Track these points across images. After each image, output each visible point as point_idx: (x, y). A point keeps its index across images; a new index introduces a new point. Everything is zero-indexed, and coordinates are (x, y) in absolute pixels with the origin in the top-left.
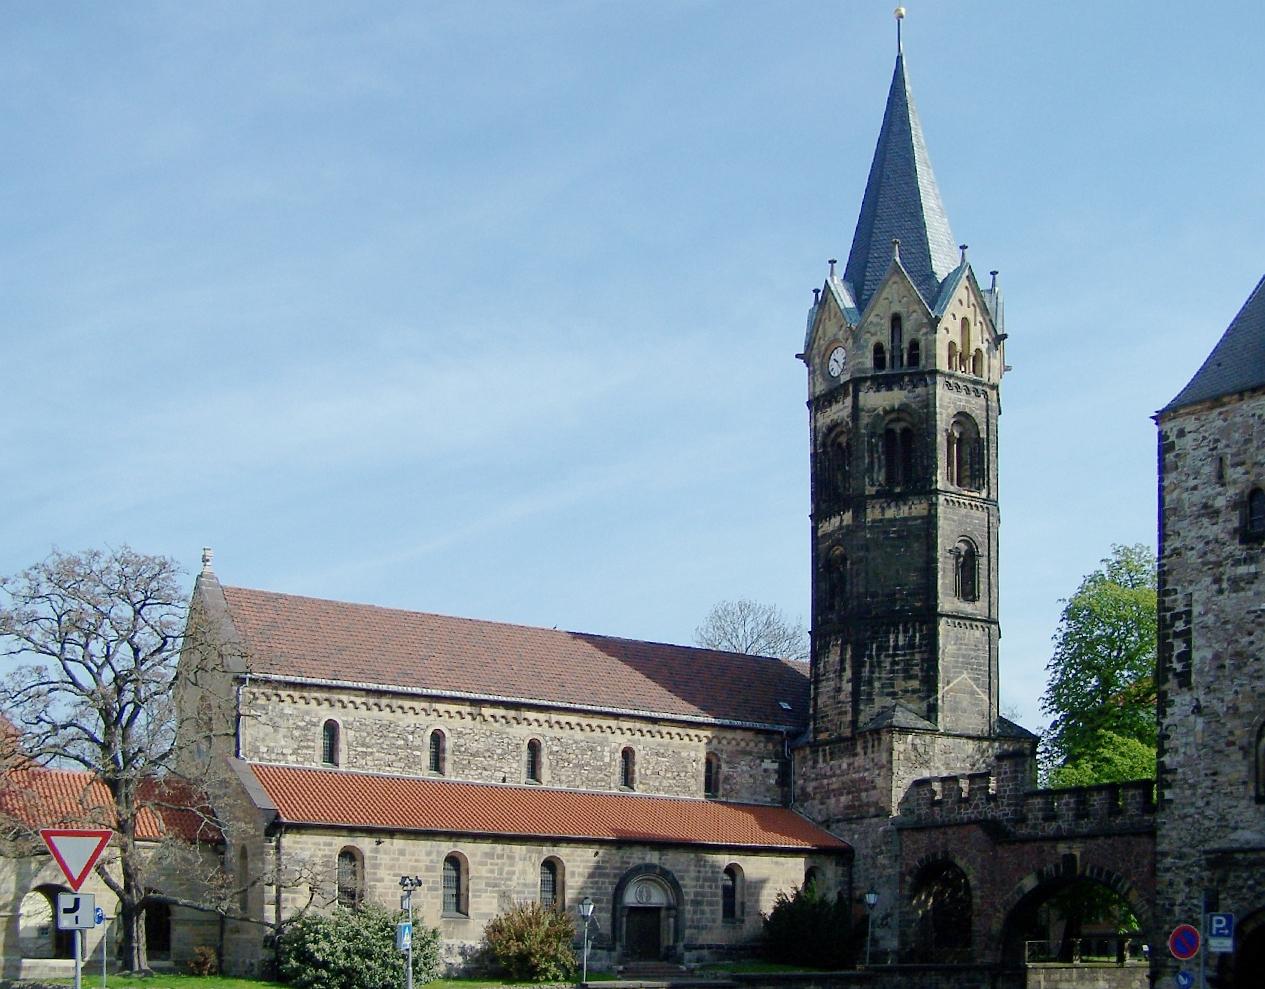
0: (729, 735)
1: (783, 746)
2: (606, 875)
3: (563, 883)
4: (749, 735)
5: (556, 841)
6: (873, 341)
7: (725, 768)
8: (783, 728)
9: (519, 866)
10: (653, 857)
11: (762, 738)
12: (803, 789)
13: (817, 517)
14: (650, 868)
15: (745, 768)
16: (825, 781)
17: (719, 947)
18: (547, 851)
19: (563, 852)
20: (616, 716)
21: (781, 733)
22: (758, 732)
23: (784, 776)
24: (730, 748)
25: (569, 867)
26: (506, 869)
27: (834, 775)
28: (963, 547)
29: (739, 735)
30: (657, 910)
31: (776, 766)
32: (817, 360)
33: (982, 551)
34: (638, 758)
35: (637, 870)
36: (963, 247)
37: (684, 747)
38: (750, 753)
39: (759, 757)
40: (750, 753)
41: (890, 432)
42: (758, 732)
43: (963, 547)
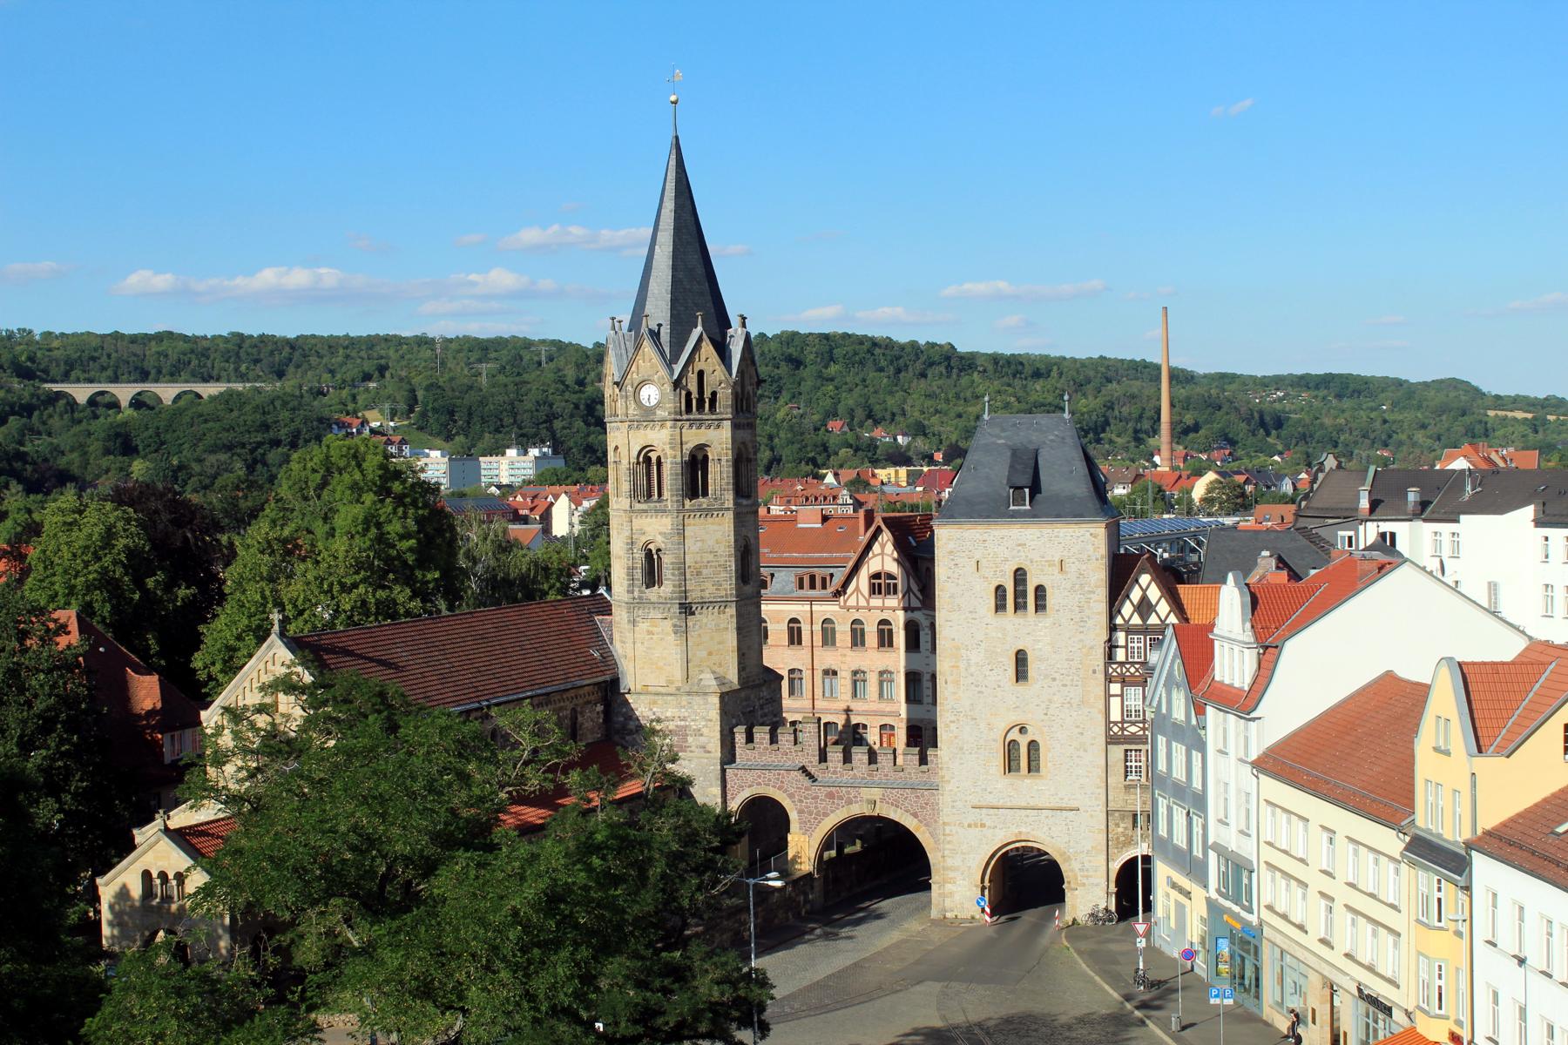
32: (629, 388)
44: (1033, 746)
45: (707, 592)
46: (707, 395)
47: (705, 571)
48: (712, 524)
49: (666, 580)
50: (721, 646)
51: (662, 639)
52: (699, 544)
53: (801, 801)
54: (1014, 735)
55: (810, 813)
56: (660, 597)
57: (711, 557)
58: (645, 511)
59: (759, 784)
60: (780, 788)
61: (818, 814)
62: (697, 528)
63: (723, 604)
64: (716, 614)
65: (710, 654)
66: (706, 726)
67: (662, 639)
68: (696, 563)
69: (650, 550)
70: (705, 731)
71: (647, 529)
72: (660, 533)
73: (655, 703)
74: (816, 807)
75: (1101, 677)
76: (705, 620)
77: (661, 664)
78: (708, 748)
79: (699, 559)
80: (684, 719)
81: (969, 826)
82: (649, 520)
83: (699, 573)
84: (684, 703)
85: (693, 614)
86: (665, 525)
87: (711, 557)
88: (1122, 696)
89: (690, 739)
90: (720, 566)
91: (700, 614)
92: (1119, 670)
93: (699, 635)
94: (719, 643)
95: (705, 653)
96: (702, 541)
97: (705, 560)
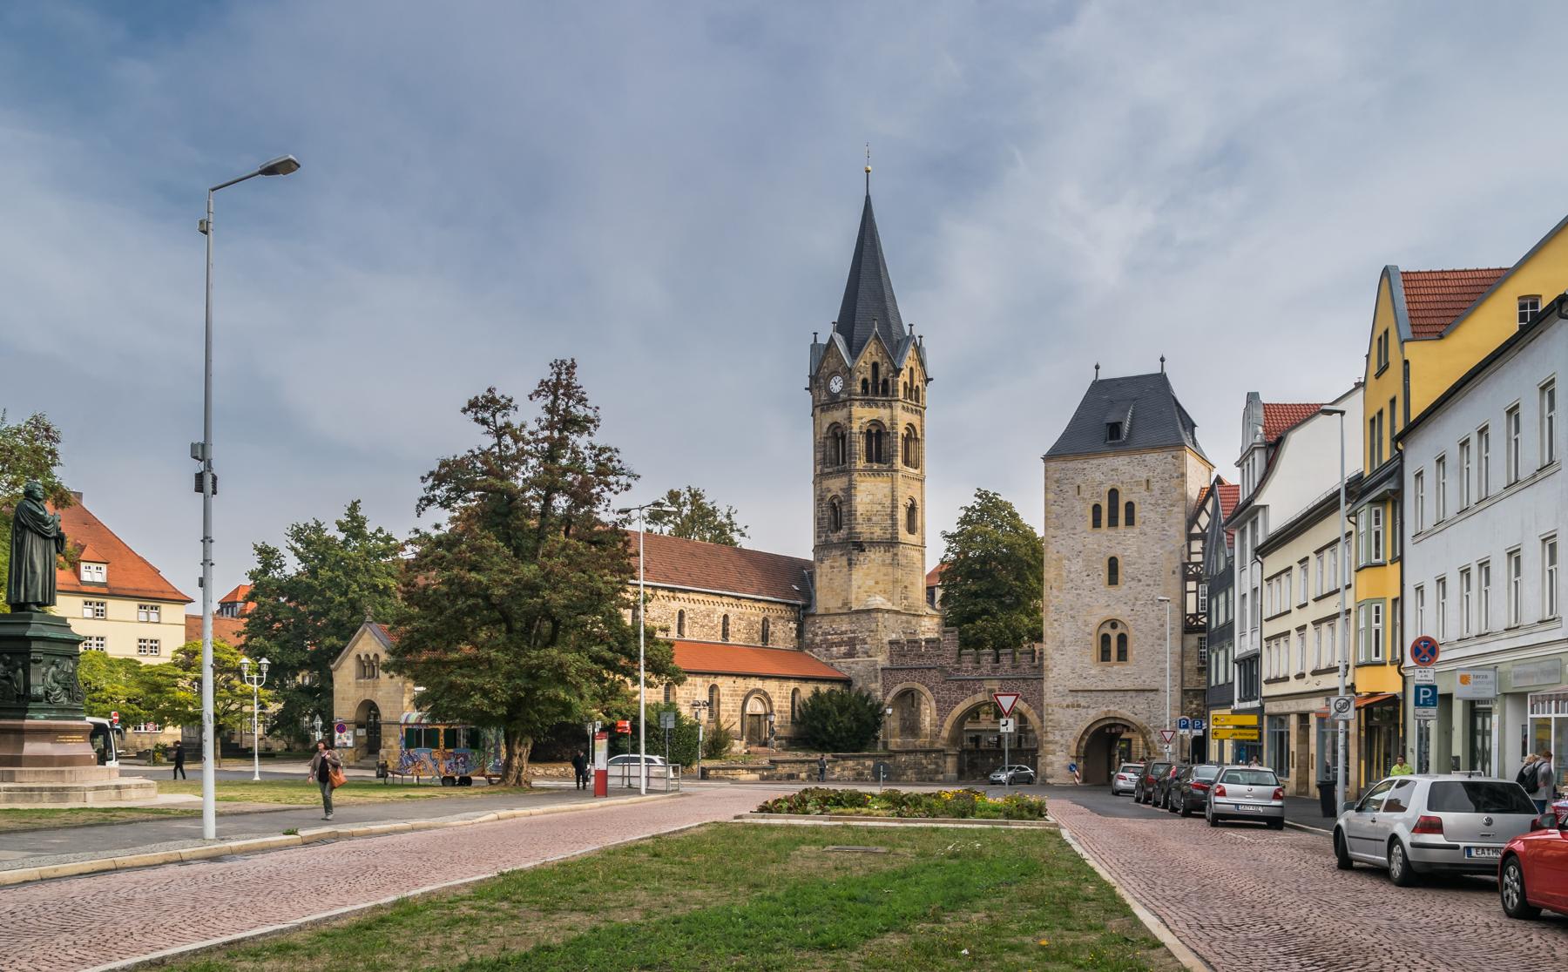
0: (774, 607)
1: (799, 613)
2: (737, 695)
3: (719, 700)
4: (783, 607)
5: (716, 674)
6: (862, 377)
7: (772, 628)
8: (800, 602)
9: (699, 690)
10: (758, 684)
11: (789, 608)
12: (812, 641)
13: (820, 477)
14: (758, 691)
16: (829, 637)
17: (790, 738)
18: (712, 680)
19: (719, 681)
20: (721, 595)
21: (798, 605)
22: (788, 604)
23: (800, 632)
24: (774, 614)
25: (722, 690)
26: (693, 692)
27: (836, 633)
28: (910, 502)
29: (778, 607)
30: (759, 715)
31: (795, 626)
32: (822, 381)
33: (918, 502)
34: (731, 621)
35: (753, 692)
37: (752, 614)
38: (783, 618)
40: (783, 618)
41: (869, 431)
42: (788, 604)
43: (910, 502)
44: (1122, 639)
45: (876, 534)
46: (880, 381)
47: (874, 518)
51: (840, 571)
52: (870, 497)
53: (938, 693)
54: (1107, 630)
55: (945, 702)
57: (879, 508)
58: (831, 473)
59: (907, 681)
60: (923, 683)
61: (951, 703)
65: (877, 583)
66: (869, 636)
70: (869, 640)
71: (832, 487)
73: (834, 621)
74: (950, 697)
75: (1178, 576)
76: (873, 556)
78: (870, 653)
80: (854, 632)
81: (1068, 706)
83: (869, 520)
85: (864, 551)
87: (879, 508)
88: (1197, 592)
89: (858, 647)
92: (1194, 569)
93: (868, 568)
94: (885, 575)
95: (872, 583)
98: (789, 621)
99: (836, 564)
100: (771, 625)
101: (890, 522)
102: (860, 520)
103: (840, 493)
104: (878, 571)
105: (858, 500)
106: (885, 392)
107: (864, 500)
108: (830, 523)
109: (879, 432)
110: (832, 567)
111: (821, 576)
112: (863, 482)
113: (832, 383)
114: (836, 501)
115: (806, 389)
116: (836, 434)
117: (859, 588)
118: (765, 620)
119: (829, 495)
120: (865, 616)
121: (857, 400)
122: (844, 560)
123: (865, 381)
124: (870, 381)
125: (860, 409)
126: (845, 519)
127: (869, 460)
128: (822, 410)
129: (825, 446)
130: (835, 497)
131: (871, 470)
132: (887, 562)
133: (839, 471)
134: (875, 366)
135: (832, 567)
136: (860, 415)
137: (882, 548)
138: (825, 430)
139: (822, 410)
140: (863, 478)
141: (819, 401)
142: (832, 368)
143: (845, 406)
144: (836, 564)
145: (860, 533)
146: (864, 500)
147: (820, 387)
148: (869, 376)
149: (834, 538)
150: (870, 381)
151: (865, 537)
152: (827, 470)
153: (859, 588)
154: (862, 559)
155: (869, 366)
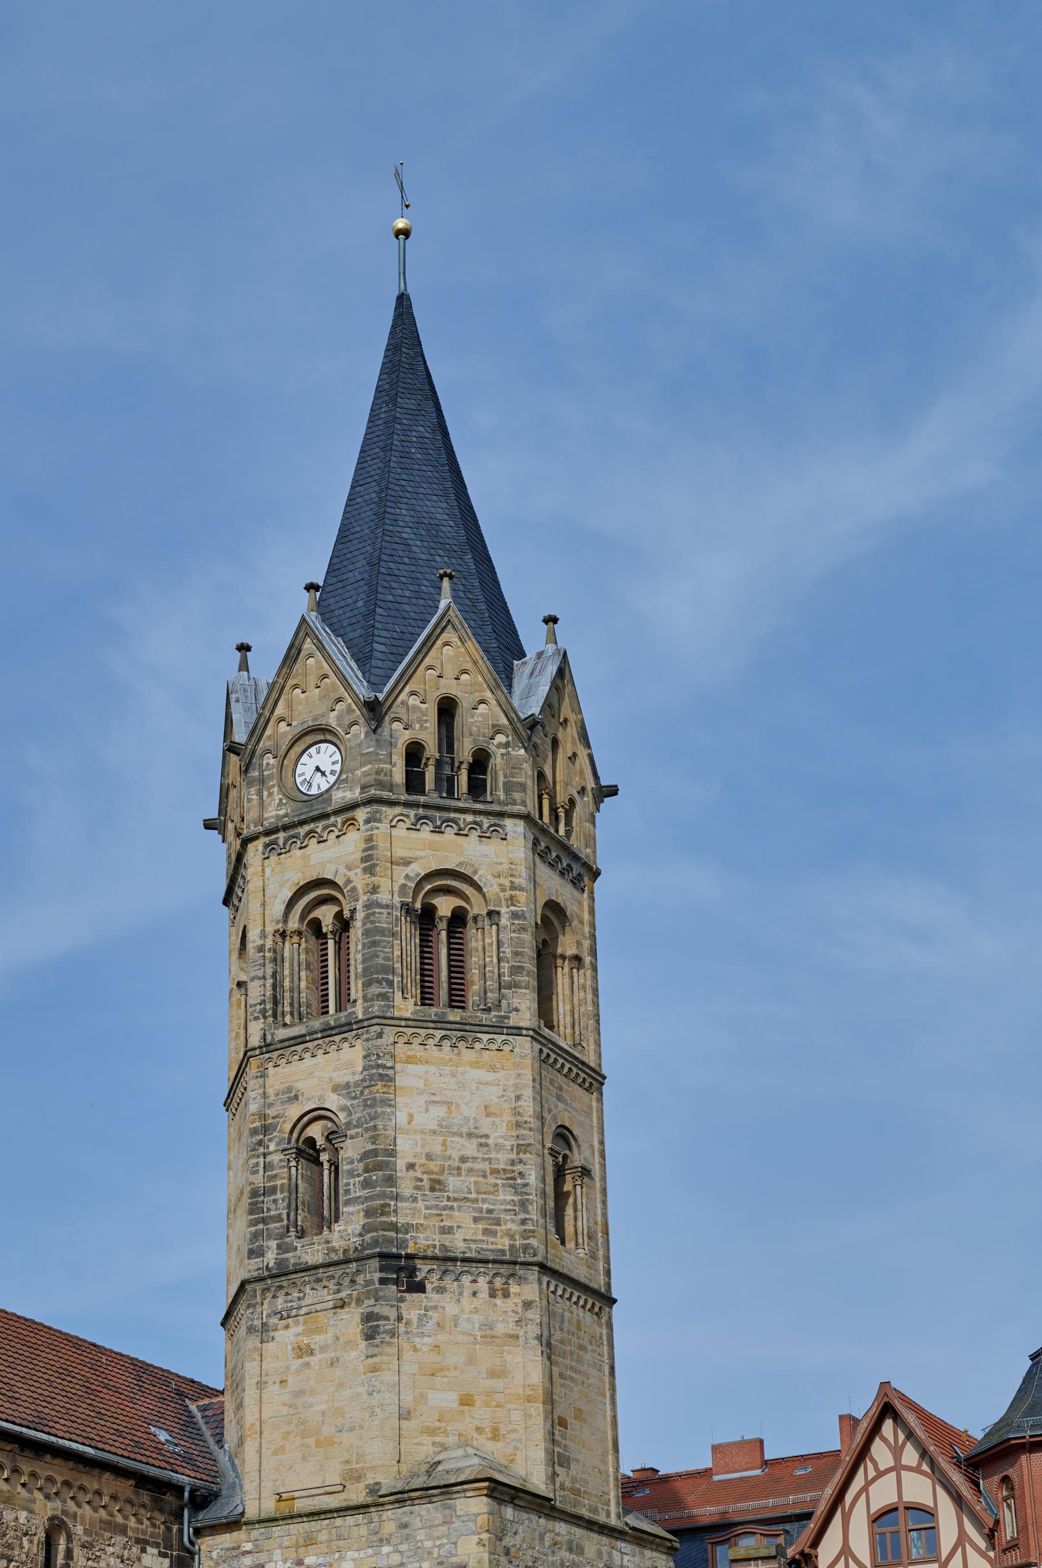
11: (145, 1497)
15: (112, 1561)
21: (178, 1489)
36: (551, 620)
39: (138, 1541)
40: (123, 1530)
45: (459, 1235)
46: (465, 751)
47: (453, 1182)
48: (476, 1065)
49: (347, 1203)
50: (497, 1384)
51: (333, 1363)
56: (334, 1250)
57: (470, 1148)
58: (299, 1040)
62: (432, 1069)
63: (504, 1270)
64: (484, 1295)
65: (466, 1401)
67: (333, 1363)
68: (429, 1157)
69: (311, 1142)
72: (336, 1089)
73: (310, 1541)
76: (451, 1309)
77: (327, 1430)
79: (438, 1149)
82: (308, 1061)
83: (437, 1185)
84: (389, 1527)
85: (419, 1288)
86: (351, 1064)
87: (470, 1148)
90: (495, 1172)
91: (441, 1290)
94: (493, 1374)
95: (449, 1400)
96: (449, 1104)
97: (456, 1155)
98: (143, 1544)
99: (317, 1340)
100: (77, 1552)
101: (506, 1196)
102: (406, 1187)
103: (333, 1102)
104: (471, 1361)
105: (401, 1117)
106: (477, 788)
107: (419, 1120)
108: (293, 1206)
109: (458, 919)
110: (303, 1351)
111: (261, 1385)
112: (410, 1060)
113: (306, 767)
114: (316, 1131)
115: (209, 825)
116: (316, 926)
117: (404, 1415)
118: (55, 1527)
119: (294, 1112)
120: (426, 1512)
121: (392, 803)
122: (351, 1320)
123: (414, 753)
124: (432, 750)
125: (400, 831)
126: (352, 1185)
127: (426, 998)
128: (270, 847)
129: (277, 960)
130: (318, 1114)
131: (440, 1023)
132: (501, 1329)
133: (327, 1031)
134: (447, 709)
135: (303, 1351)
136: (399, 853)
137: (482, 1283)
138: (278, 908)
139: (270, 847)
140: (416, 1049)
141: (260, 821)
142: (303, 718)
143: (351, 822)
144: (317, 1340)
145: (408, 1228)
146: (419, 1120)
147: (262, 781)
148: (429, 736)
149: (312, 1253)
150: (432, 750)
151: (421, 1241)
152: (282, 1033)
153: (404, 1415)
154: (412, 1314)
155: (431, 710)
